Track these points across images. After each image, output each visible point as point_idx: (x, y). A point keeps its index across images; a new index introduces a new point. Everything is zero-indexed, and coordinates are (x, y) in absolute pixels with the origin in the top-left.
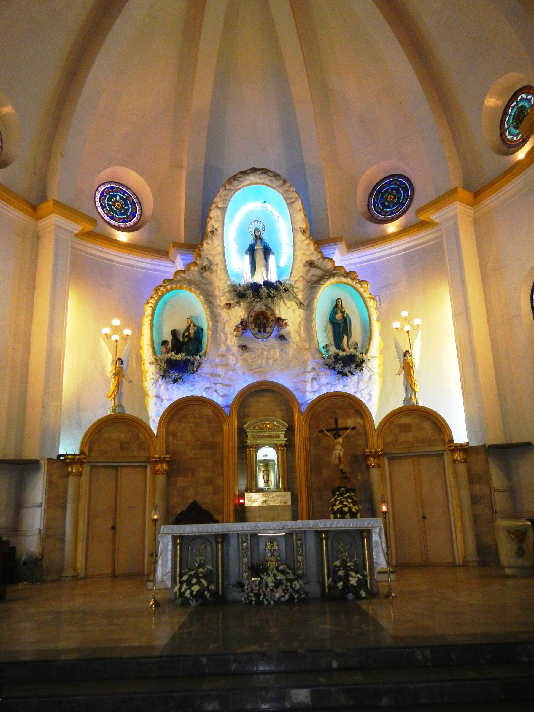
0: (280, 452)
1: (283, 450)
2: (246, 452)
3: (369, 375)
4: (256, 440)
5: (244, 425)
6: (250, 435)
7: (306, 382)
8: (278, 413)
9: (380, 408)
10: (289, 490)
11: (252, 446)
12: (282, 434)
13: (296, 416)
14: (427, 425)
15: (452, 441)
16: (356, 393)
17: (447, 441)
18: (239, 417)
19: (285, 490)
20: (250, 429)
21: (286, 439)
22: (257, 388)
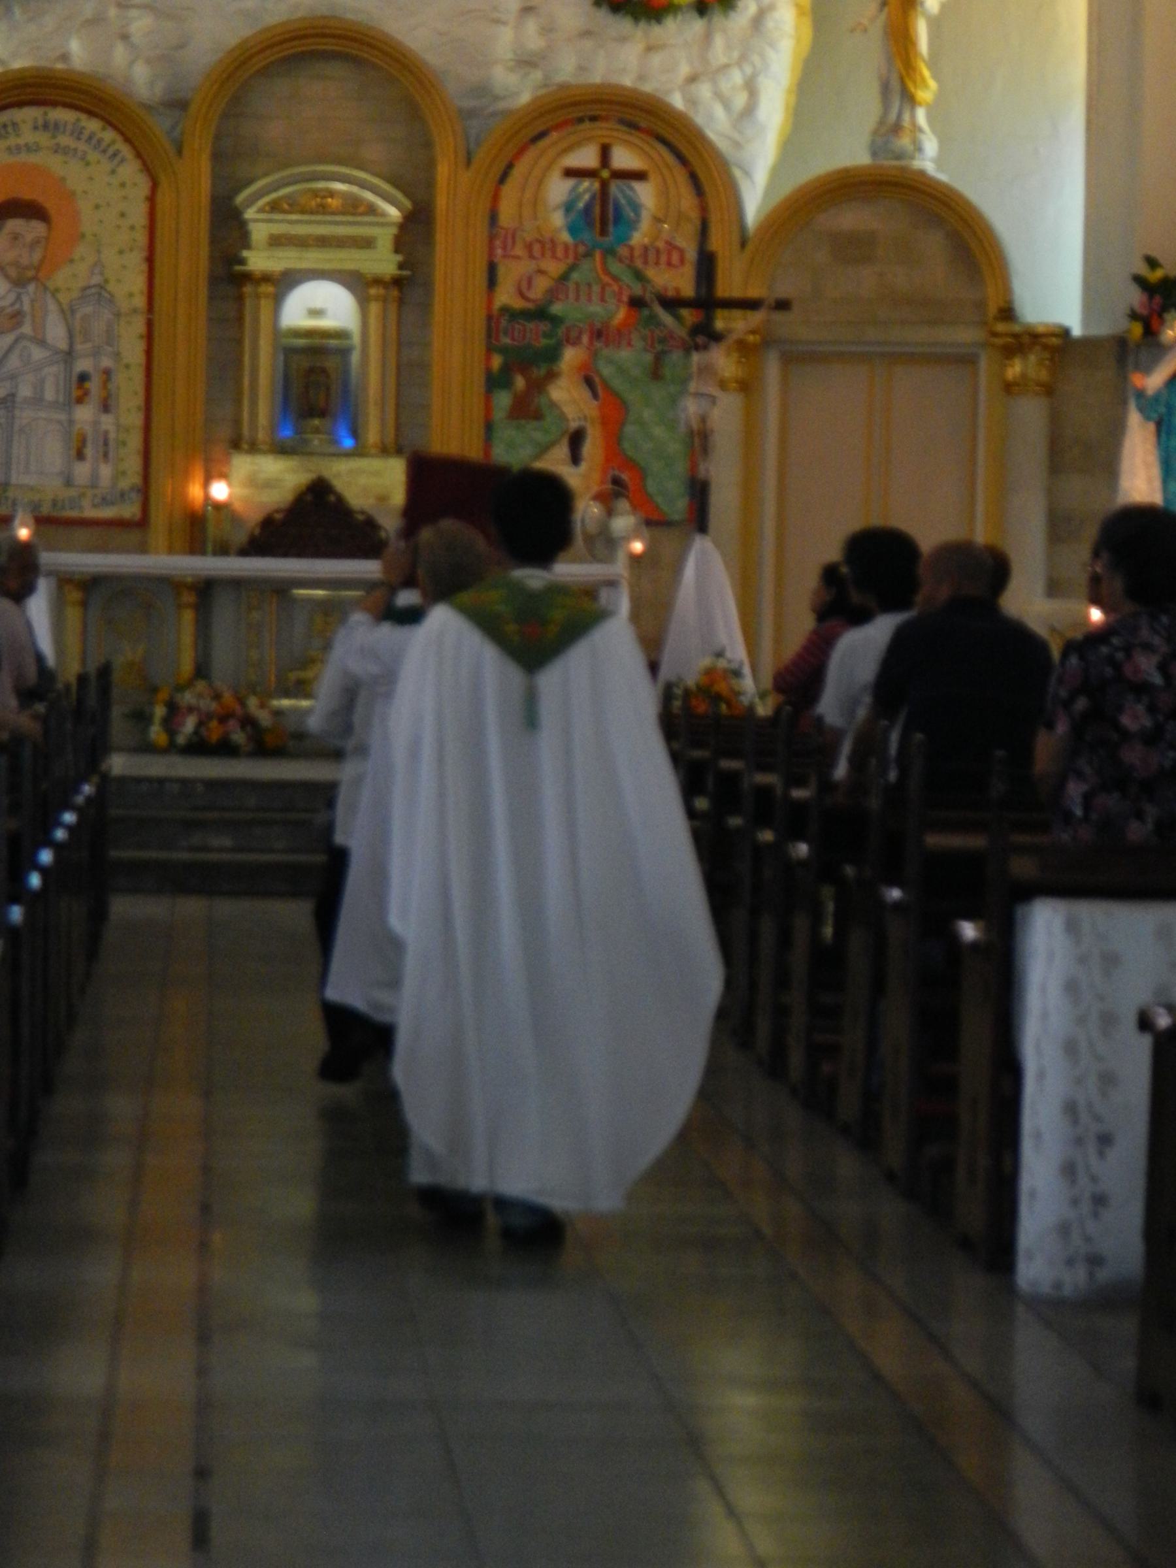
0: (374, 308)
1: (384, 300)
2: (240, 299)
3: (752, 9)
4: (281, 253)
5: (237, 190)
6: (259, 231)
7: (497, 21)
8: (374, 152)
9: (790, 147)
10: (399, 451)
11: (266, 278)
12: (385, 237)
13: (443, 171)
14: (933, 244)
15: (1008, 313)
16: (693, 79)
17: (992, 310)
18: (217, 157)
19: (384, 451)
20: (261, 210)
21: (399, 258)
22: (298, 47)
